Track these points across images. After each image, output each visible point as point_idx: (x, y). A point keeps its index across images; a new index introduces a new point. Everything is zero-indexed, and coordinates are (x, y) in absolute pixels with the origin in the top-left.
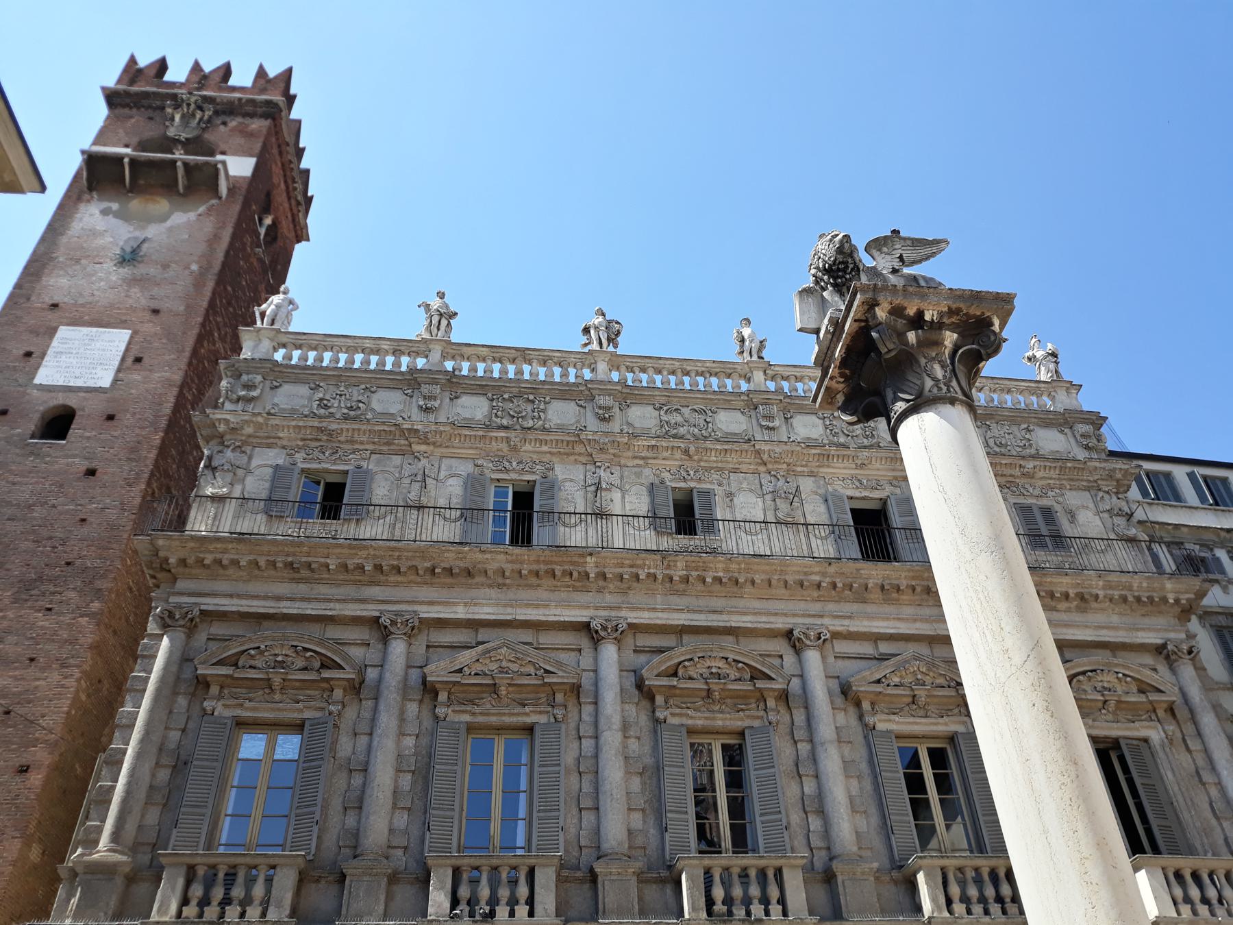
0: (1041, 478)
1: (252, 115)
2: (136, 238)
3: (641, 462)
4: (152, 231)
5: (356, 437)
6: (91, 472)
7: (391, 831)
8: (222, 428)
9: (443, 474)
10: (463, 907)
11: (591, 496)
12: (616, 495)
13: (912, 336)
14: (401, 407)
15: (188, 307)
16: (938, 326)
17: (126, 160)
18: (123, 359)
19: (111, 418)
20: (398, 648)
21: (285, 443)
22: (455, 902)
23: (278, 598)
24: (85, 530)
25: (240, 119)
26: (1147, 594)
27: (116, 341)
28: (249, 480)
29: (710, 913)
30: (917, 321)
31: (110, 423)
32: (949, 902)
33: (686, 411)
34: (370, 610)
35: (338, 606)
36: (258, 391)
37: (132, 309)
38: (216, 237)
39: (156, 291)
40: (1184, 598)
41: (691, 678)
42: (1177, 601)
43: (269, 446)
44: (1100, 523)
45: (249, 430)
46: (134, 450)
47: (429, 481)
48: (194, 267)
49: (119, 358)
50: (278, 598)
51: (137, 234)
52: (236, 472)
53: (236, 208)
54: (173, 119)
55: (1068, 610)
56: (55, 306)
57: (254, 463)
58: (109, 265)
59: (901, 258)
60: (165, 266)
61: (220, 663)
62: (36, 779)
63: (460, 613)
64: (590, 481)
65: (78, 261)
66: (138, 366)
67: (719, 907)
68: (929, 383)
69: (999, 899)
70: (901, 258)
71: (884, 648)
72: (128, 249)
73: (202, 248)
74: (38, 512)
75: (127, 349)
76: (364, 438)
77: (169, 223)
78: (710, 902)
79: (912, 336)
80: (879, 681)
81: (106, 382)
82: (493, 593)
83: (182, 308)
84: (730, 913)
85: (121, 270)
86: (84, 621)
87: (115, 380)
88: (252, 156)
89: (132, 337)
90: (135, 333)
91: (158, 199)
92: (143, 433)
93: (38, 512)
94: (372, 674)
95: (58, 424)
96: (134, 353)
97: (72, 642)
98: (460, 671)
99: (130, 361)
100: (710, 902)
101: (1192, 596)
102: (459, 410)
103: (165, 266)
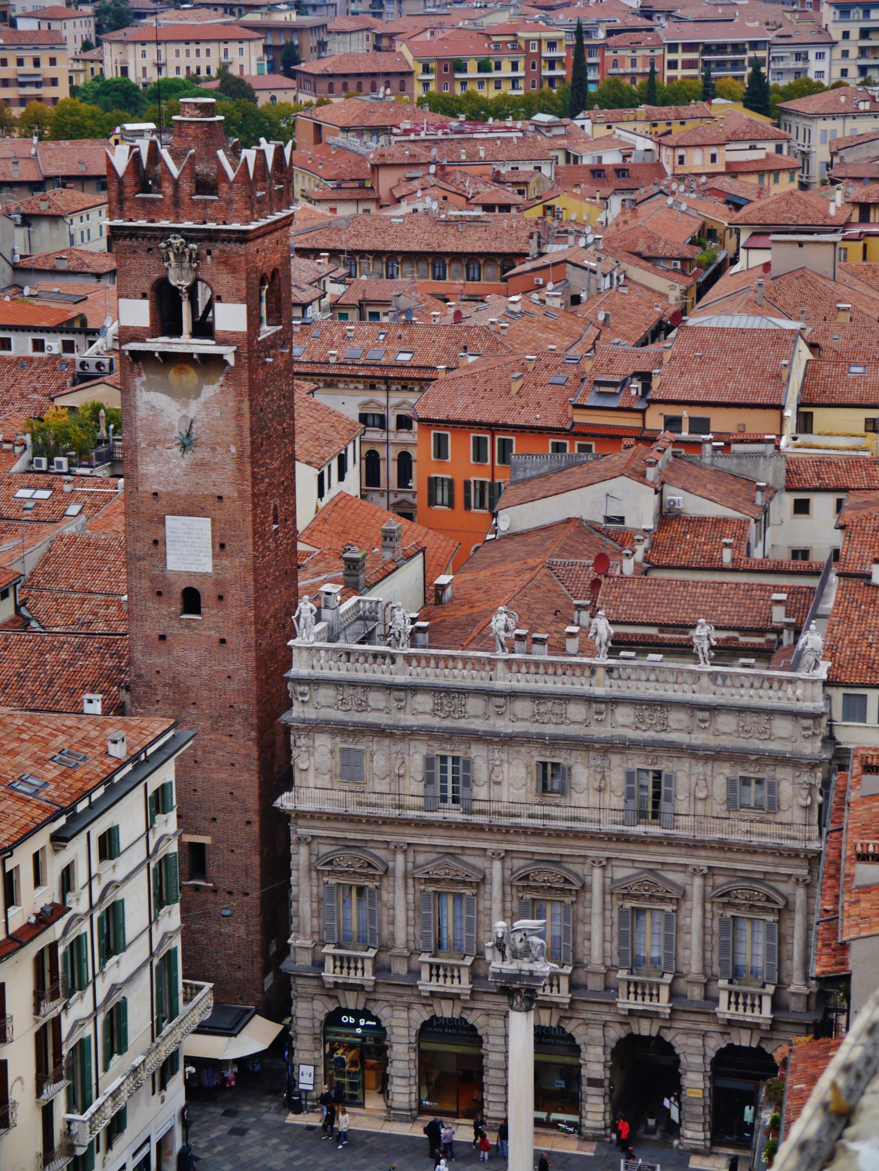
1: (230, 240)
2: (185, 417)
4: (194, 408)
6: (223, 641)
7: (407, 934)
9: (412, 751)
10: (434, 978)
12: (505, 766)
17: (157, 355)
18: (213, 547)
19: (221, 598)
20: (400, 858)
22: (431, 975)
24: (234, 685)
25: (219, 246)
27: (202, 527)
28: (316, 754)
33: (550, 704)
37: (205, 497)
38: (239, 415)
39: (214, 476)
41: (535, 880)
46: (241, 624)
47: (406, 757)
48: (233, 449)
51: (184, 412)
52: (310, 751)
53: (245, 375)
54: (168, 259)
56: (155, 494)
57: (317, 743)
58: (176, 450)
60: (214, 449)
62: (256, 828)
63: (426, 841)
65: (154, 446)
72: (185, 434)
73: (232, 423)
74: (205, 671)
75: (213, 537)
77: (202, 399)
81: (209, 569)
85: (185, 456)
86: (250, 743)
87: (214, 566)
88: (241, 301)
89: (213, 525)
90: (213, 521)
91: (187, 367)
92: (240, 598)
93: (205, 671)
94: (391, 864)
95: (191, 600)
96: (218, 540)
97: (247, 756)
99: (218, 546)
102: (417, 706)
103: (214, 449)
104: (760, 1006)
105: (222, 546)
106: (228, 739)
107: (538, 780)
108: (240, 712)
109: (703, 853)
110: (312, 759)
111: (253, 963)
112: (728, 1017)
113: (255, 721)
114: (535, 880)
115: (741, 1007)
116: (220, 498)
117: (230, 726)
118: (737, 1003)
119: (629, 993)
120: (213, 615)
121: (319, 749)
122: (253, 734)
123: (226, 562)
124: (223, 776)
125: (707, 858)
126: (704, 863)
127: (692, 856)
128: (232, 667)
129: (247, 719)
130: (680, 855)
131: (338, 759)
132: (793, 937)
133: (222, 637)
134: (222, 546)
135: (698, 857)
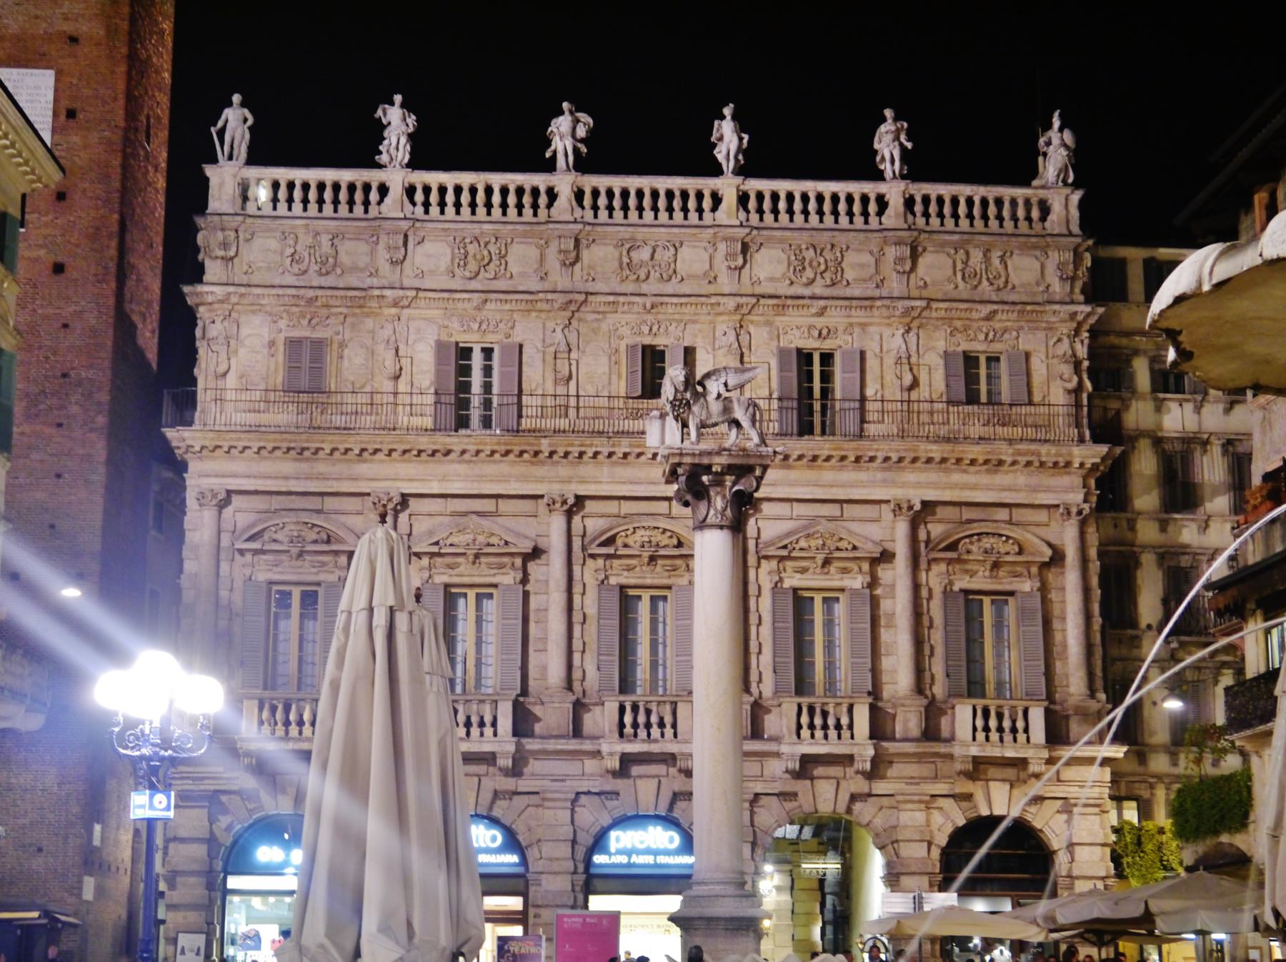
0: (1000, 320)
3: (600, 316)
5: (332, 302)
6: (59, 268)
8: (210, 299)
11: (550, 358)
13: (705, 478)
14: (366, 259)
15: (108, 31)
16: (722, 474)
21: (268, 309)
23: (286, 478)
26: (1054, 459)
28: (242, 351)
29: (621, 735)
30: (707, 469)
31: (63, 204)
32: (799, 727)
34: (363, 487)
35: (335, 483)
36: (234, 249)
37: (48, 38)
40: (1089, 463)
41: (626, 546)
42: (1082, 465)
43: (254, 312)
44: (1044, 371)
45: (234, 299)
49: (50, 113)
50: (286, 478)
55: (977, 472)
57: (245, 331)
59: (726, 384)
61: (251, 538)
64: (548, 341)
66: (72, 123)
67: (628, 730)
68: (712, 512)
69: (838, 727)
70: (726, 384)
71: (800, 509)
75: (56, 100)
76: (338, 303)
78: (622, 725)
79: (705, 478)
80: (785, 547)
82: (462, 468)
83: (102, 33)
84: (636, 735)
86: (93, 436)
89: (57, 80)
96: (65, 103)
98: (437, 543)
99: (63, 117)
100: (622, 725)
101: (1098, 460)
104: (1026, 730)
105: (71, 114)
106: (53, 431)
107: (631, 373)
108: (79, 383)
109: (910, 476)
110: (233, 361)
111: (66, 838)
112: (974, 751)
113: (104, 397)
114: (626, 546)
115: (994, 736)
116: (74, 40)
117: (61, 408)
118: (986, 729)
119: (799, 727)
120: (46, 225)
121: (247, 342)
122: (101, 420)
123: (76, 139)
124: (39, 495)
125: (918, 485)
126: (916, 497)
127: (893, 484)
128: (71, 309)
129: (90, 395)
130: (872, 484)
131: (280, 357)
132: (1064, 619)
133: (60, 259)
134: (71, 114)
135: (904, 485)
